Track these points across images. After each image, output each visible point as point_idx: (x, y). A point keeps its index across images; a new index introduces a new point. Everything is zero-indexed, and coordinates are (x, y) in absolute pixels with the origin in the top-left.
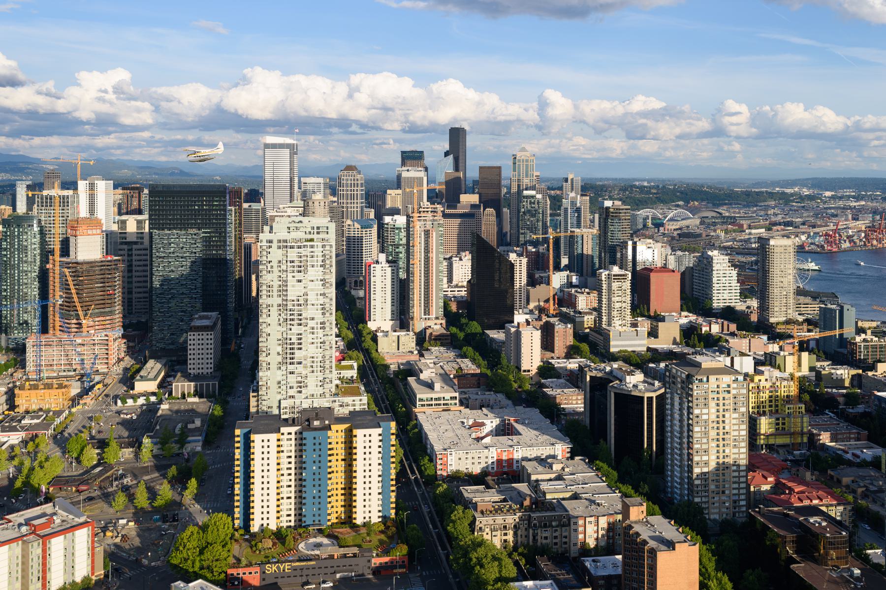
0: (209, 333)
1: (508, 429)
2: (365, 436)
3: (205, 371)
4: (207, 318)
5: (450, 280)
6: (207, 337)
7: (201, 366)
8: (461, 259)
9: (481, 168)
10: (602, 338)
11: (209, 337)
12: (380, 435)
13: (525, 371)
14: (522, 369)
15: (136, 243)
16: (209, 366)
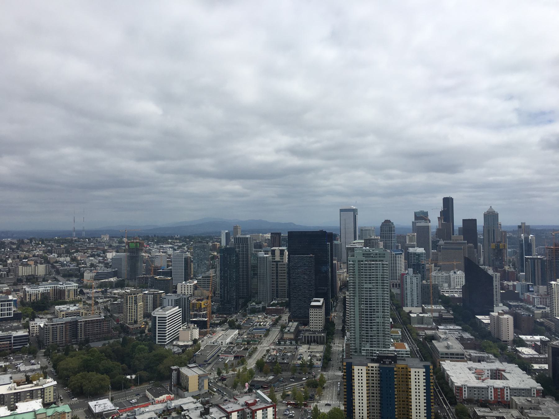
0: (320, 309)
1: (499, 376)
2: (415, 372)
3: (318, 329)
4: (319, 301)
5: (449, 286)
6: (319, 311)
7: (316, 327)
8: (455, 273)
9: (463, 220)
10: (553, 324)
11: (320, 311)
12: (424, 372)
13: (504, 341)
14: (502, 340)
15: (279, 261)
16: (320, 327)
